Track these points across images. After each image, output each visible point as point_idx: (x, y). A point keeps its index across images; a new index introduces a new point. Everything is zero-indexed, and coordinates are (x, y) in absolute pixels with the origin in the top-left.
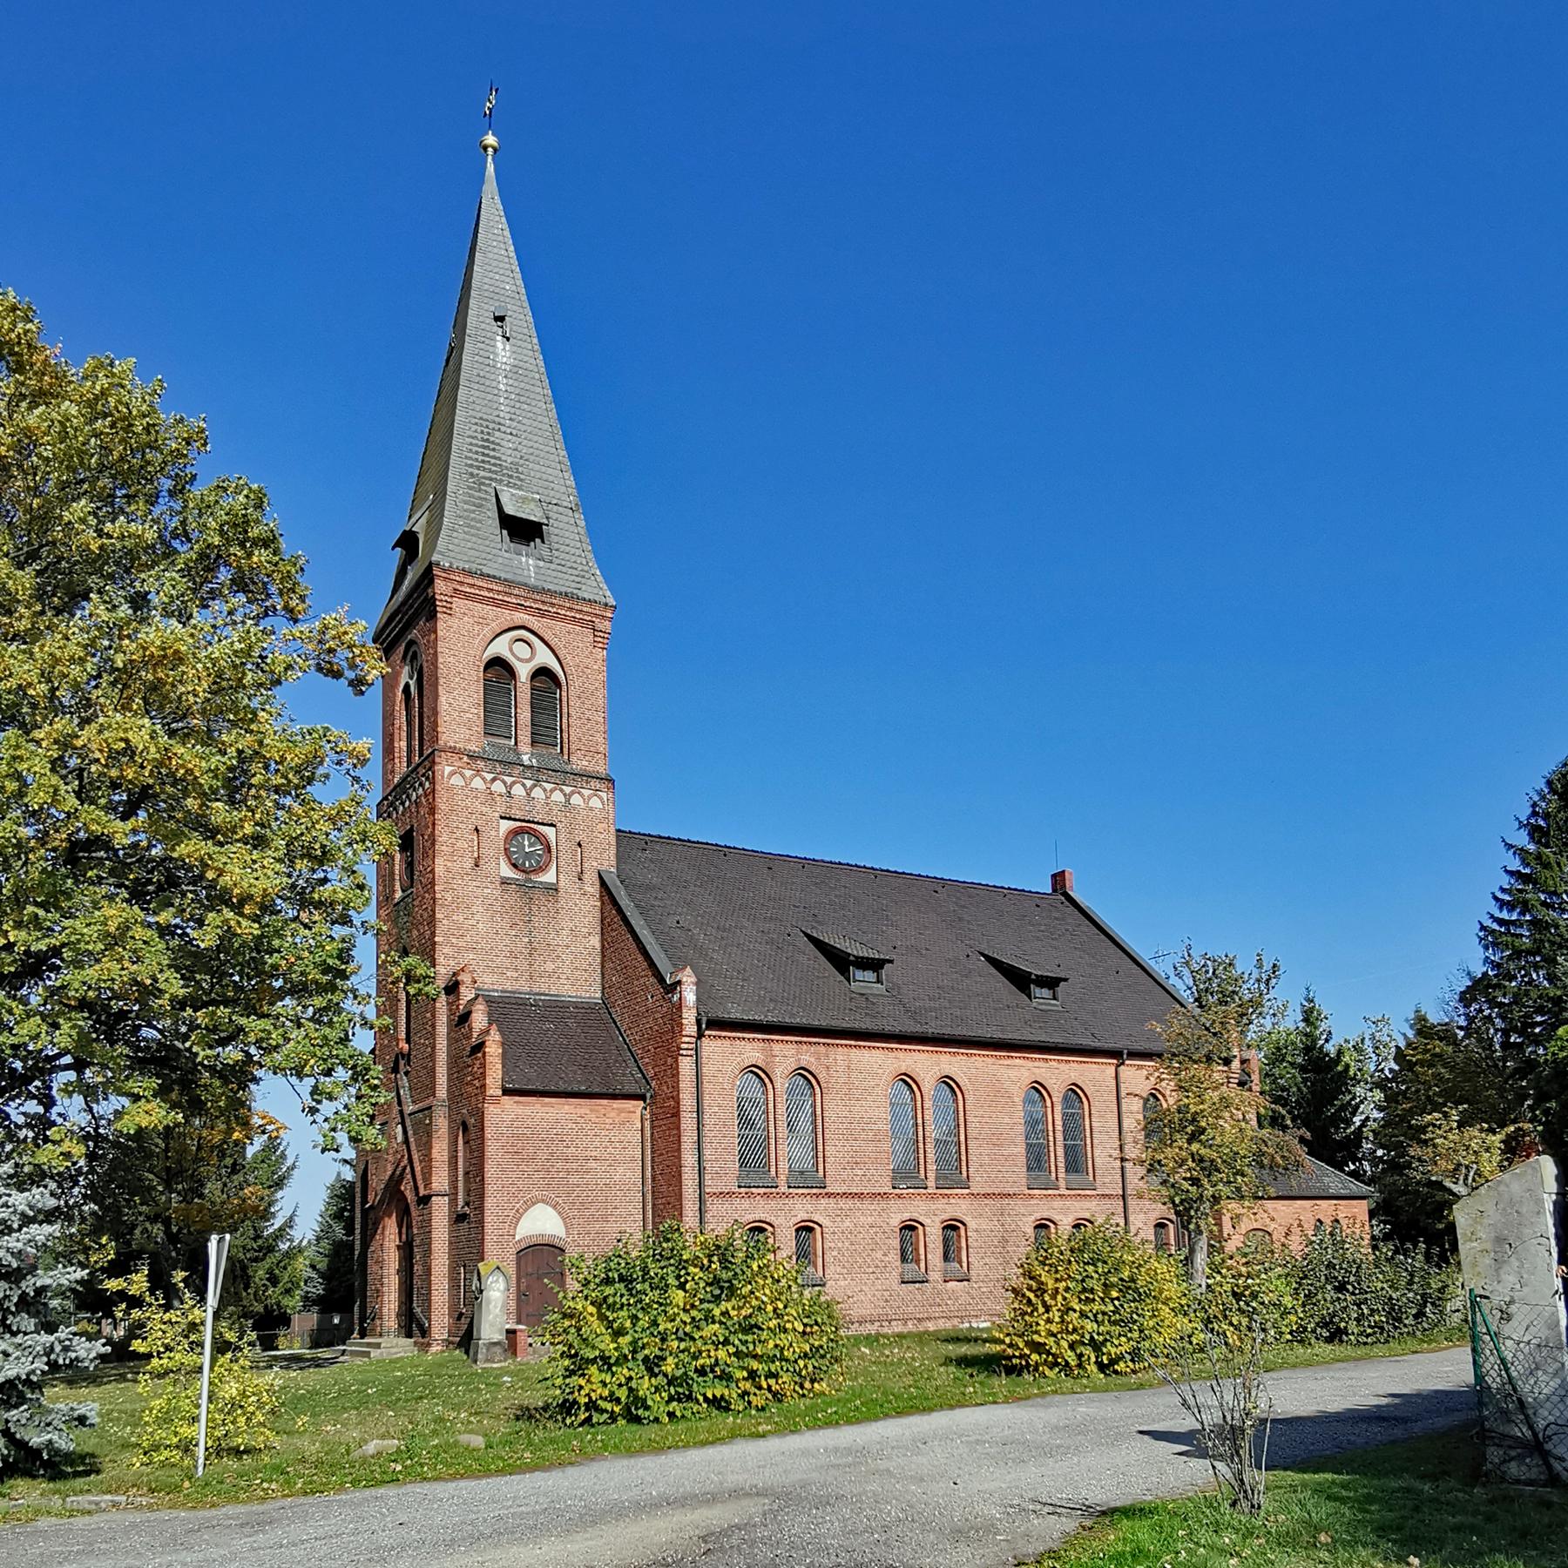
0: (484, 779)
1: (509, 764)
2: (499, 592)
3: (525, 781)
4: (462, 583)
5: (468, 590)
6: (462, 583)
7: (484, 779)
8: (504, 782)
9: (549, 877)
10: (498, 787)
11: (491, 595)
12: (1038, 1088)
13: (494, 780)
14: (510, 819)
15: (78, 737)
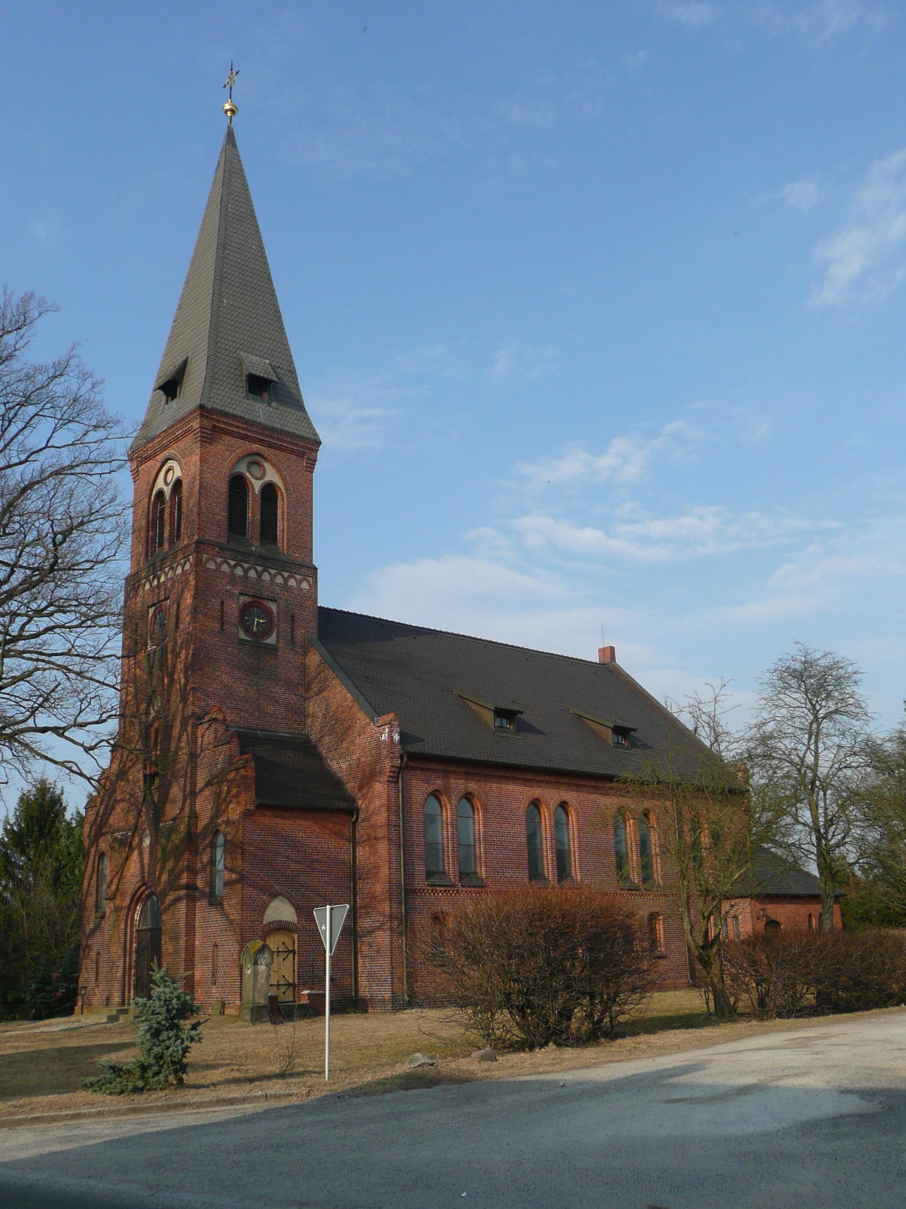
0: (229, 564)
1: (244, 556)
2: (243, 429)
3: (257, 567)
4: (218, 421)
5: (222, 426)
6: (218, 421)
7: (229, 564)
8: (243, 567)
9: (272, 640)
10: (239, 571)
11: (238, 430)
12: (536, 803)
13: (235, 566)
14: (246, 595)
15: (51, 857)
